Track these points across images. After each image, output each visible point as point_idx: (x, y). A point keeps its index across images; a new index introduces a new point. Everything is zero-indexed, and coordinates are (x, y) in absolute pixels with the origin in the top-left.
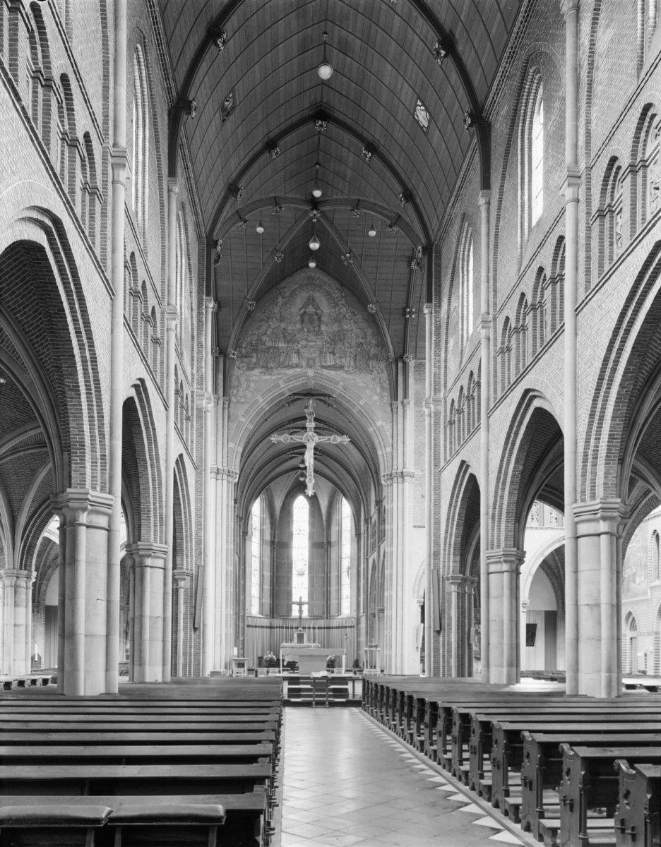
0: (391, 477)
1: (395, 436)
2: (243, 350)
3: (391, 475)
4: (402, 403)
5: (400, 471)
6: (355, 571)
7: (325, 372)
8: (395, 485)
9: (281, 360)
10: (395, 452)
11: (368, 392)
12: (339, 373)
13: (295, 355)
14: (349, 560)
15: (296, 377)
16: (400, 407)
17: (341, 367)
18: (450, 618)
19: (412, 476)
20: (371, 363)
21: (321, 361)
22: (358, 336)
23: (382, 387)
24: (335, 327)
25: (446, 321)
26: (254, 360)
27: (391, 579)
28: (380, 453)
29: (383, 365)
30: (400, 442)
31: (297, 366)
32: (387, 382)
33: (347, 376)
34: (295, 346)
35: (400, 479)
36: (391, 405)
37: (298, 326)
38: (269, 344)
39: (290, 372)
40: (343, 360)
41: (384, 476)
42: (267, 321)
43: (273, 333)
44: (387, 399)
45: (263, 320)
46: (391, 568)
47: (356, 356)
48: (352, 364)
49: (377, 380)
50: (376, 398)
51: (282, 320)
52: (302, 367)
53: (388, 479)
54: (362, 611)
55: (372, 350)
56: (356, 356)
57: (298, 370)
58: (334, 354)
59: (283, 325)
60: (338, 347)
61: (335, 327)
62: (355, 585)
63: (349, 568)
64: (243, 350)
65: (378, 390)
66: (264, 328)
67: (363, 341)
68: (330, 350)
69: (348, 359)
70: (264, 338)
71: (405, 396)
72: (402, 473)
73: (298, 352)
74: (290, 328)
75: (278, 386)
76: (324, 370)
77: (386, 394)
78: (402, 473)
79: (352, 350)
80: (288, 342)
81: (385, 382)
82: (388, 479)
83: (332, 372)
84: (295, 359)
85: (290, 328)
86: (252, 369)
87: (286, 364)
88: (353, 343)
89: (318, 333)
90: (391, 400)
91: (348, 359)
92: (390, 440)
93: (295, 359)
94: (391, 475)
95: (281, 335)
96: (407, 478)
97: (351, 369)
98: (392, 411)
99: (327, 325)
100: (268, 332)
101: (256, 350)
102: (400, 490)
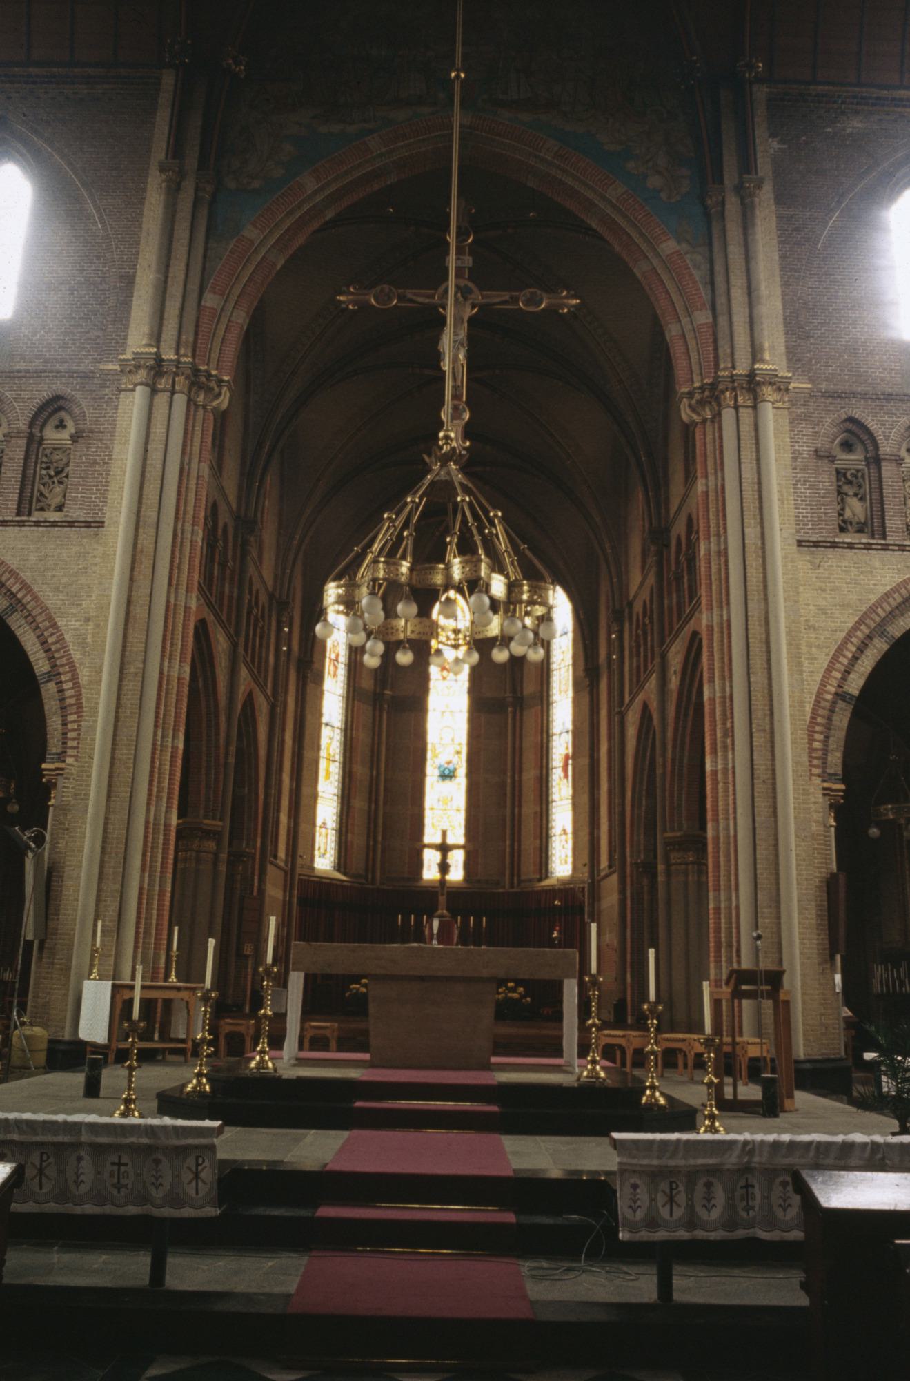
0: (712, 395)
1: (719, 279)
5: (741, 369)
6: (585, 761)
8: (728, 415)
10: (722, 321)
11: (631, 165)
14: (568, 738)
19: (781, 387)
27: (728, 714)
28: (672, 331)
30: (738, 294)
41: (690, 395)
46: (727, 674)
53: (701, 403)
54: (604, 862)
62: (585, 798)
63: (567, 757)
72: (752, 375)
78: (752, 375)
82: (701, 403)
92: (705, 293)
94: (713, 386)
96: (767, 391)
102: (746, 428)
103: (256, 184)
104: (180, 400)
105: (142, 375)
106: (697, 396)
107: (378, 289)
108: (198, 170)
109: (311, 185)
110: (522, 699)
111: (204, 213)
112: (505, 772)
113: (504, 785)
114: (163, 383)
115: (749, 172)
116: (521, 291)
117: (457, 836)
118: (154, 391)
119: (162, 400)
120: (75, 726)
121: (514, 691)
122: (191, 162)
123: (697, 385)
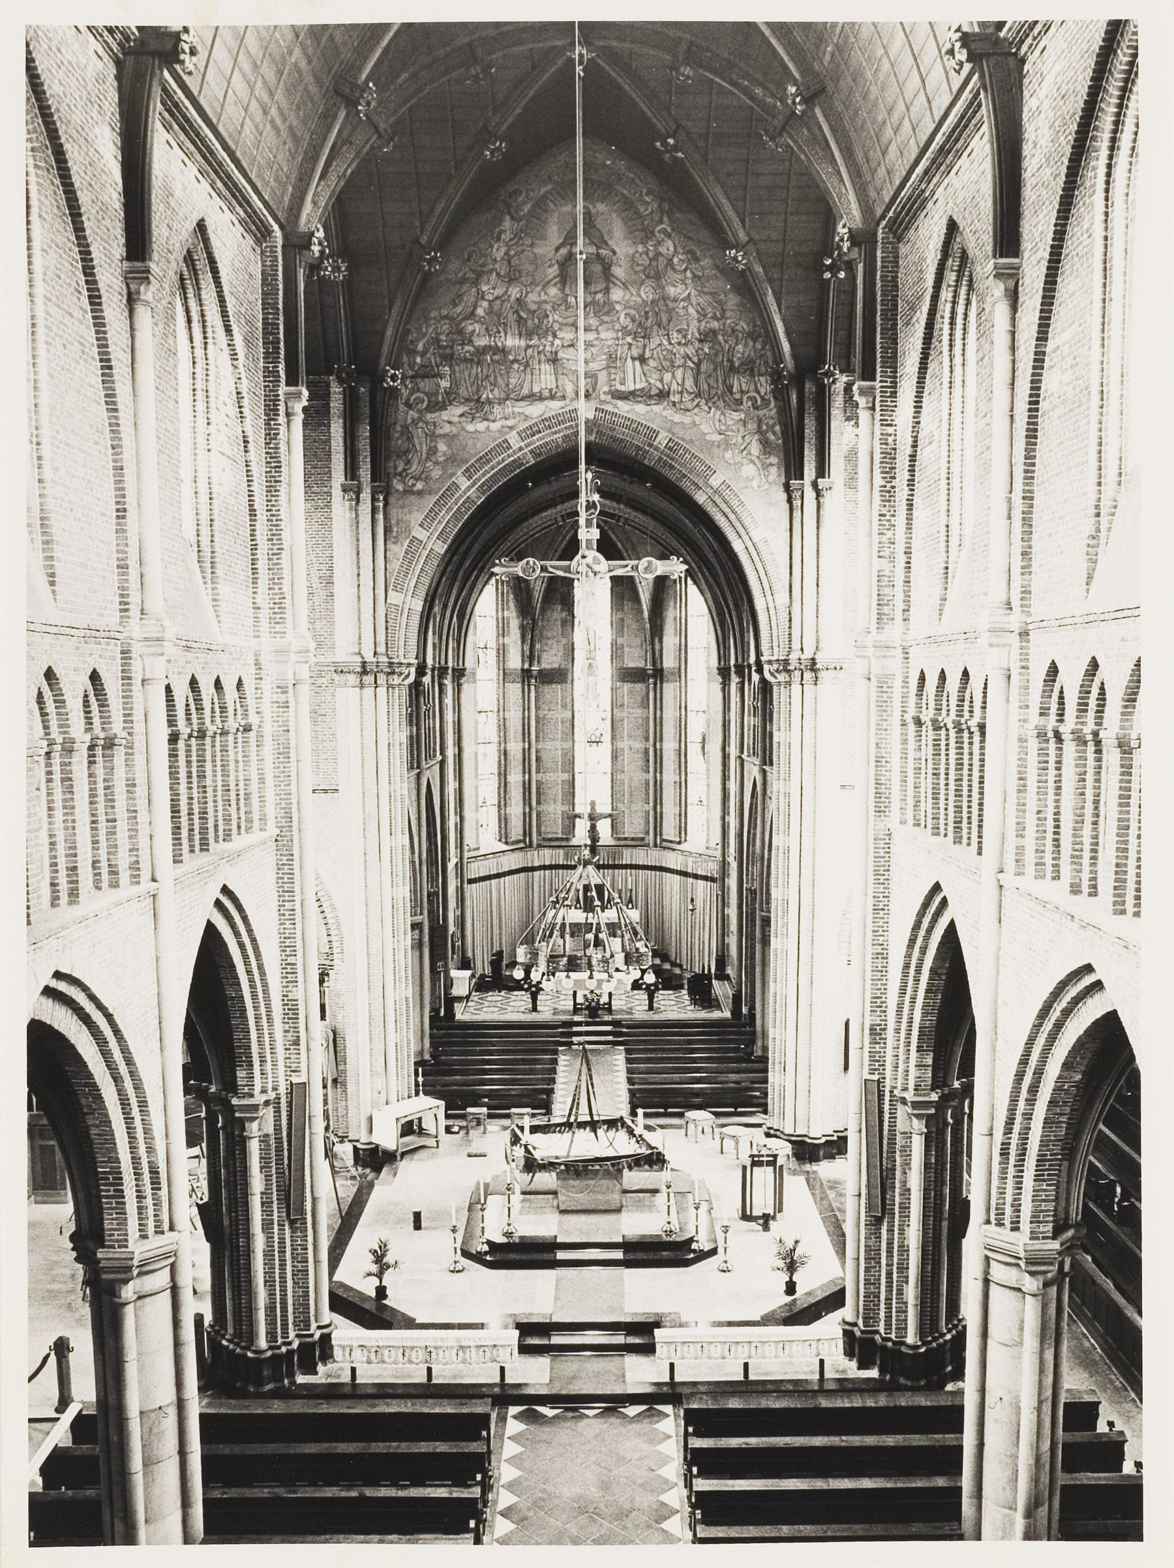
2: (418, 360)
3: (786, 662)
4: (815, 485)
5: (808, 654)
7: (623, 407)
9: (513, 381)
11: (728, 455)
12: (656, 408)
13: (546, 367)
15: (548, 422)
16: (810, 494)
17: (663, 395)
18: (907, 1191)
20: (739, 383)
21: (610, 381)
22: (702, 315)
23: (765, 443)
24: (647, 293)
25: (909, 451)
26: (445, 384)
29: (765, 385)
31: (552, 397)
32: (777, 428)
33: (677, 418)
34: (547, 344)
35: (808, 675)
36: (787, 488)
37: (553, 291)
38: (482, 342)
39: (536, 410)
40: (667, 377)
42: (476, 282)
43: (490, 311)
44: (776, 475)
45: (464, 280)
47: (698, 365)
48: (689, 384)
49: (752, 426)
50: (749, 470)
51: (512, 278)
52: (564, 398)
55: (740, 347)
56: (698, 365)
57: (555, 406)
58: (642, 359)
59: (515, 292)
60: (655, 341)
61: (647, 293)
64: (418, 360)
65: (755, 448)
66: (469, 298)
67: (715, 325)
68: (635, 352)
69: (679, 373)
70: (470, 327)
71: (822, 470)
73: (554, 360)
74: (532, 297)
75: (505, 445)
76: (620, 403)
77: (774, 460)
79: (690, 350)
80: (529, 335)
81: (771, 428)
83: (641, 408)
84: (545, 379)
85: (532, 297)
86: (444, 408)
87: (525, 391)
88: (693, 330)
89: (601, 309)
90: (788, 478)
91: (679, 373)
93: (545, 379)
95: (512, 318)
97: (686, 397)
98: (790, 501)
99: (625, 286)
100: (480, 312)
101: (449, 358)
103: (419, 486)
104: (382, 691)
105: (353, 679)
106: (775, 666)
107: (525, 561)
108: (372, 481)
109: (464, 483)
110: (662, 670)
111: (380, 517)
112: (647, 739)
113: (646, 751)
114: (369, 679)
115: (824, 477)
116: (639, 559)
117: (604, 807)
118: (362, 686)
119: (369, 691)
120: (337, 938)
121: (654, 663)
122: (365, 473)
123: (775, 658)
